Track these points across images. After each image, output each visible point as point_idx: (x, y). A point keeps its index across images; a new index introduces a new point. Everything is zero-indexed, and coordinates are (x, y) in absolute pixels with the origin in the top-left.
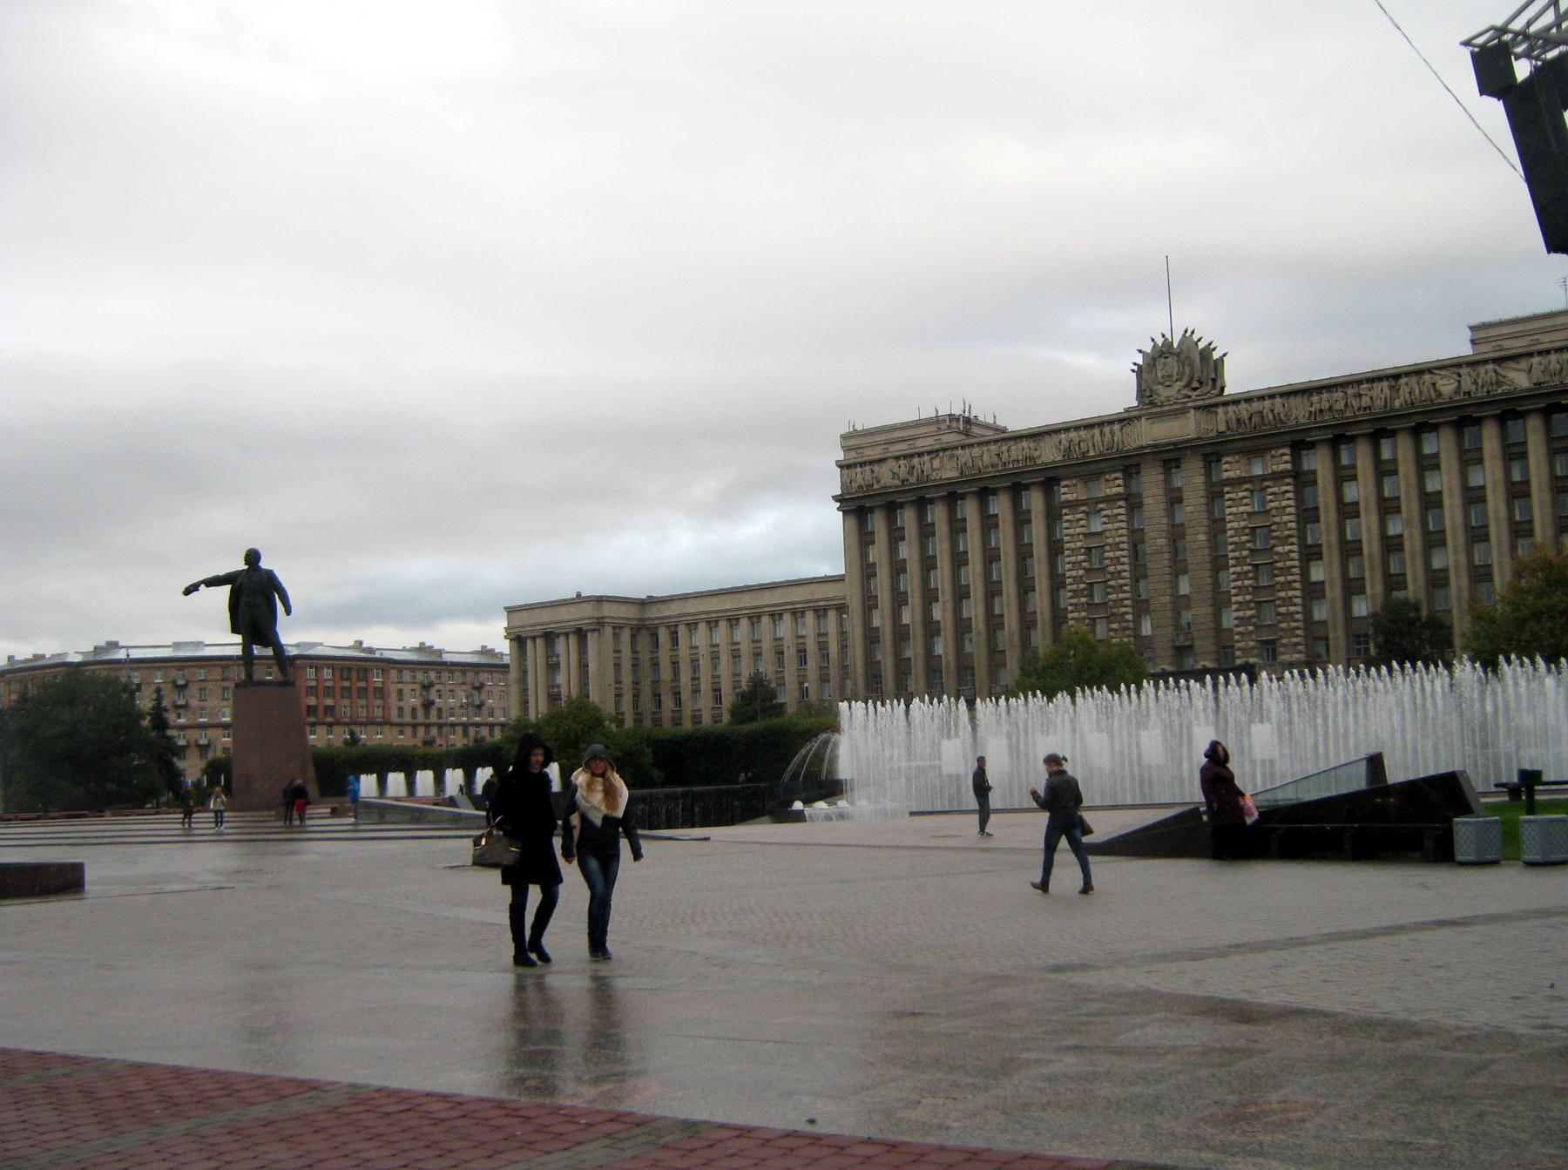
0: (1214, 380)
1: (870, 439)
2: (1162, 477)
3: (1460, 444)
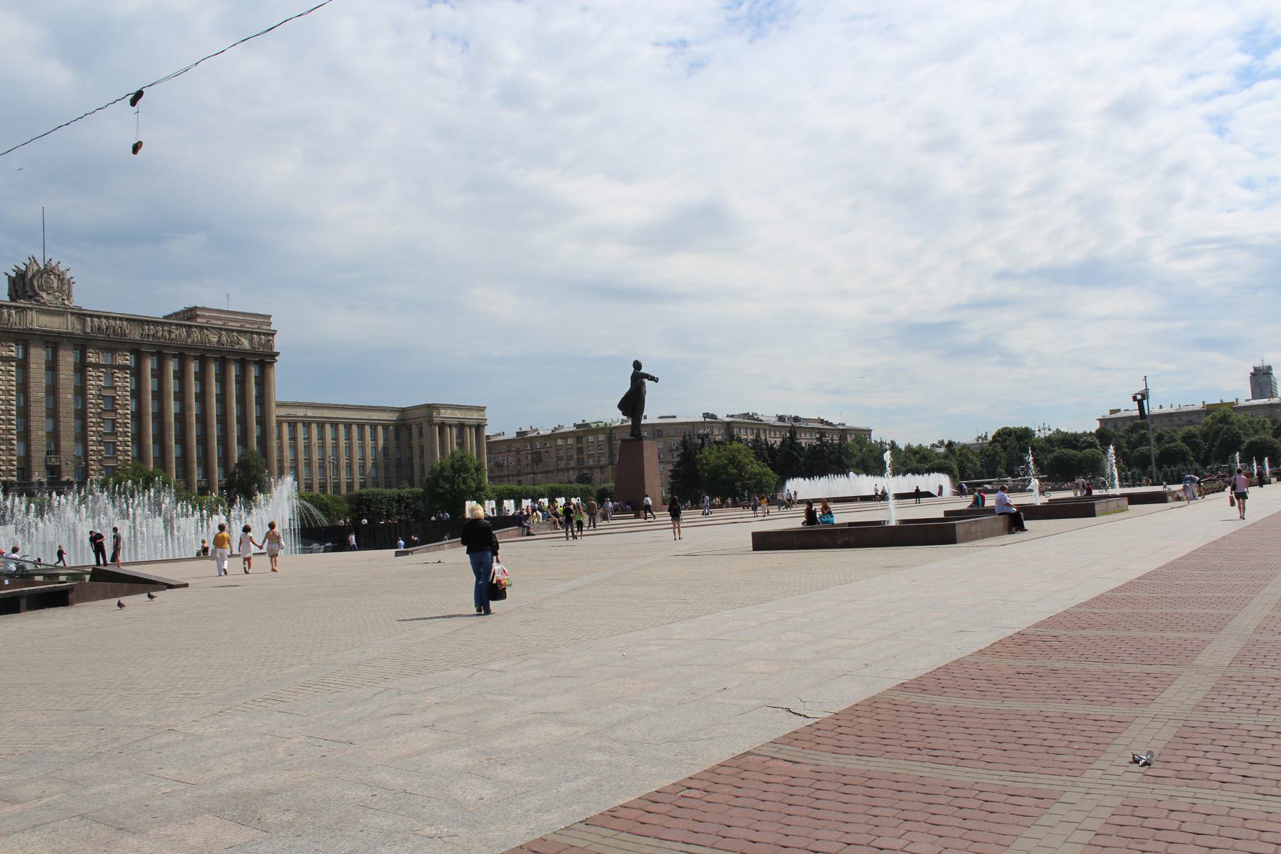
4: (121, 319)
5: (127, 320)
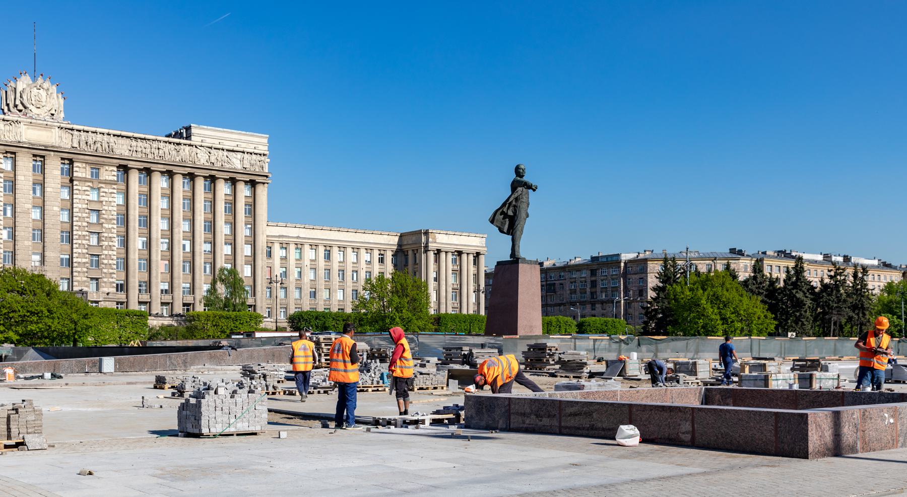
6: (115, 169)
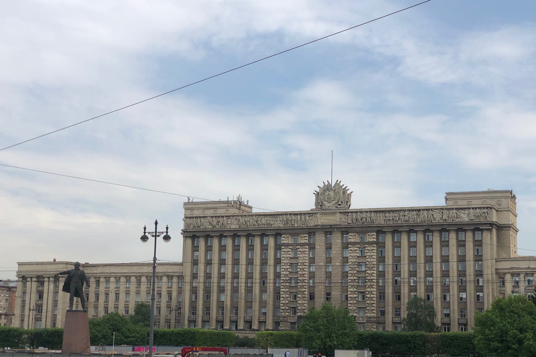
0: (347, 202)
1: (197, 206)
2: (324, 238)
3: (441, 237)
4: (371, 212)
5: (374, 212)
6: (375, 234)
